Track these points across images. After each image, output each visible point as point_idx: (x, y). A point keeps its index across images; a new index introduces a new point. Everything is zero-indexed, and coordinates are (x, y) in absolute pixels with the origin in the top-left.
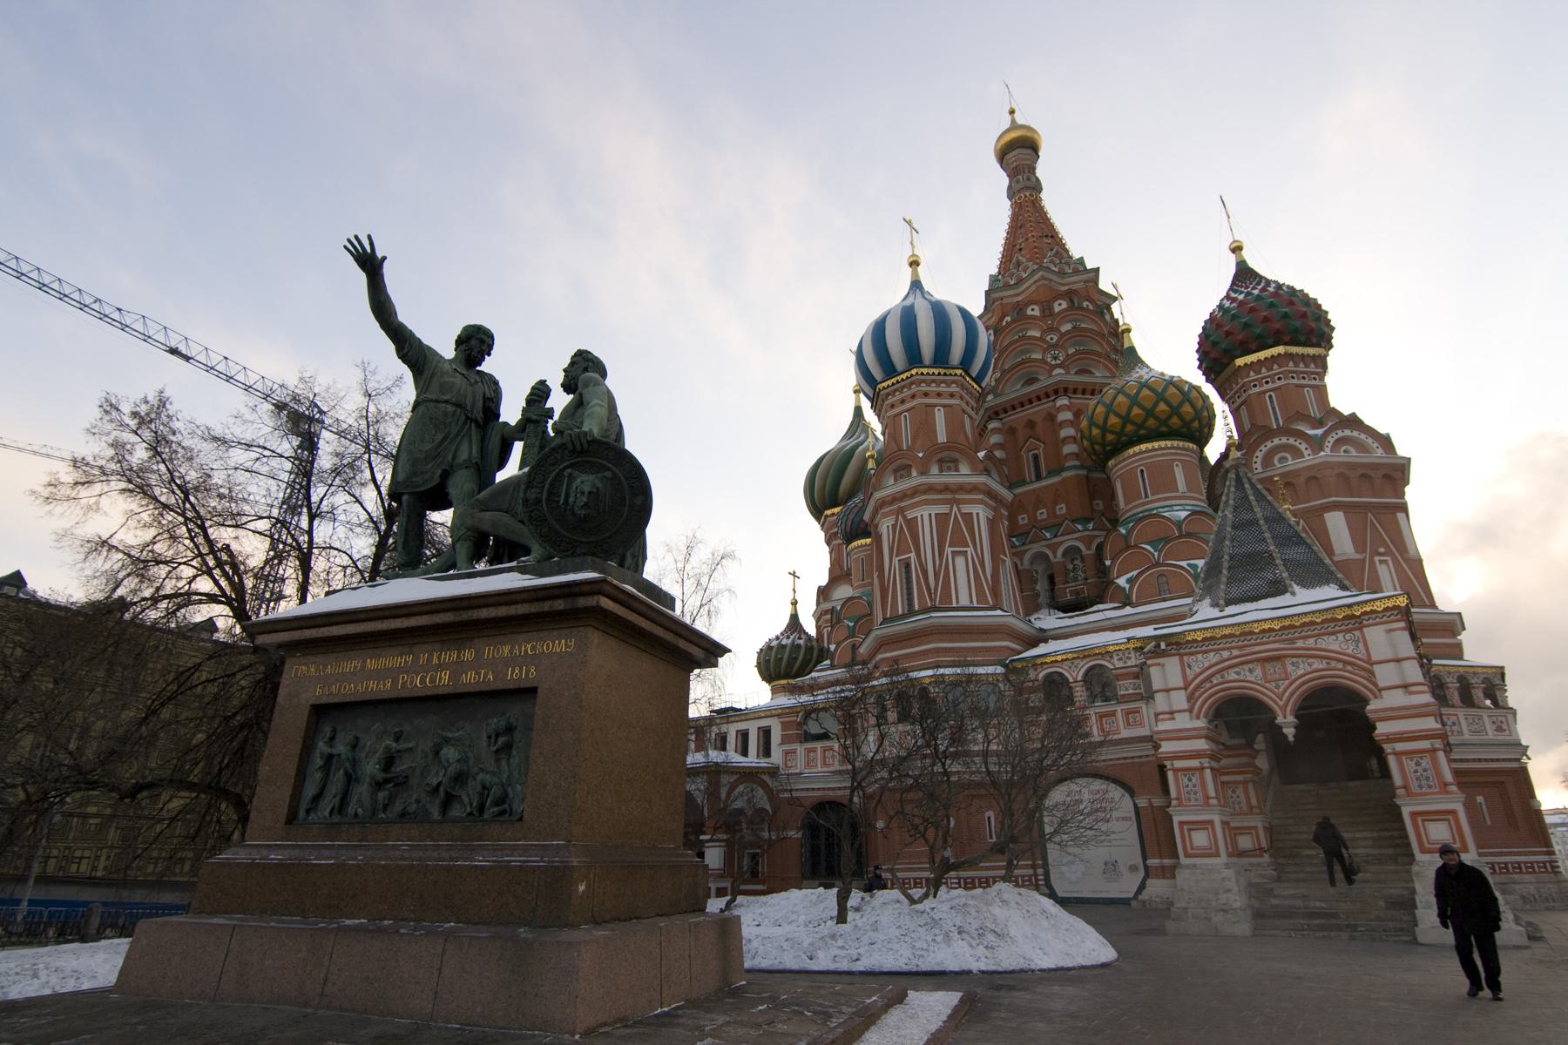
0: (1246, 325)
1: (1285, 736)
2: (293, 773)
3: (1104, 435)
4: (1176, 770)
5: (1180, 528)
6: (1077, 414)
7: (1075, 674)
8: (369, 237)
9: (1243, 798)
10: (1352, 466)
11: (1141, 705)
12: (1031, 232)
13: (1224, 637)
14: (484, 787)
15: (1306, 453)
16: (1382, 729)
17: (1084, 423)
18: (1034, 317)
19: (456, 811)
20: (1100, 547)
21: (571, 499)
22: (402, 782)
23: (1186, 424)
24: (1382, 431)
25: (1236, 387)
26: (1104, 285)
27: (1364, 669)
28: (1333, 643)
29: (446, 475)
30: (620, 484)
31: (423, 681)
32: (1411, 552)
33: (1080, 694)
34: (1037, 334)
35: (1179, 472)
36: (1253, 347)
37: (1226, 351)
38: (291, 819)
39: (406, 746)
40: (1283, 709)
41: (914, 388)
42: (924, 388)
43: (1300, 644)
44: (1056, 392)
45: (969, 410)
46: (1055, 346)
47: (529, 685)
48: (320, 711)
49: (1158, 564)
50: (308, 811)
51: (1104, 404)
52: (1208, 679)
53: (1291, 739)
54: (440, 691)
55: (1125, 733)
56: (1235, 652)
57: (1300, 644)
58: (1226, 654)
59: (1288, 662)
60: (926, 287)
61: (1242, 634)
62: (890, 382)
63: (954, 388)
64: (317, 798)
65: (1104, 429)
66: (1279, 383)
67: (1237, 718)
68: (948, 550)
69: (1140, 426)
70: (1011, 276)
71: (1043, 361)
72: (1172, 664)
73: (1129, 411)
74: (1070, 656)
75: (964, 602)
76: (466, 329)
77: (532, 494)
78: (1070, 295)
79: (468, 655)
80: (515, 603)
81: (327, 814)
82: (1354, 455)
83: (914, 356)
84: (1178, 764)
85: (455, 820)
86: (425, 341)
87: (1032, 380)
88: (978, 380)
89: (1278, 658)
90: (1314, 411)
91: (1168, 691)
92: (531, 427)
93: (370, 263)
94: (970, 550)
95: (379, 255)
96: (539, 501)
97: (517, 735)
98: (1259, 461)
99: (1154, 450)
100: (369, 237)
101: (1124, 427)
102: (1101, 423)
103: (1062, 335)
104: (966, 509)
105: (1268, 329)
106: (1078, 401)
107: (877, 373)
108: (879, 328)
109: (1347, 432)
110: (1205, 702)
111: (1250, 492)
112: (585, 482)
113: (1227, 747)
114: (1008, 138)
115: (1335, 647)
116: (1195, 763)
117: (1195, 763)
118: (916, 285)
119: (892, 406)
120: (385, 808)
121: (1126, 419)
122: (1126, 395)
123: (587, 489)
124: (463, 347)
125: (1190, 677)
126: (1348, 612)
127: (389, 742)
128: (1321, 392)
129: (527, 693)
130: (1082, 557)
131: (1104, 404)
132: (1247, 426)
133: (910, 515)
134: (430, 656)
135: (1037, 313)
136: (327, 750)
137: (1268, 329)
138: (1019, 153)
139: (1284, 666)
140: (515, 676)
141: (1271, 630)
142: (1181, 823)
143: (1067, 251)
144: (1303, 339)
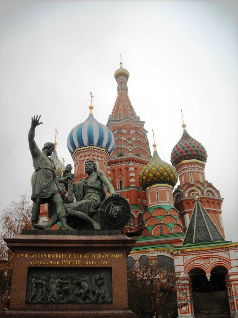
0: (186, 151)
1: (208, 280)
2: (25, 288)
3: (147, 179)
5: (167, 213)
6: (136, 169)
8: (40, 116)
10: (211, 199)
12: (123, 105)
14: (98, 294)
15: (200, 193)
16: (231, 278)
17: (141, 174)
18: (124, 133)
19: (88, 301)
20: (140, 215)
21: (112, 213)
22: (66, 293)
23: (171, 180)
24: (218, 190)
25: (181, 169)
26: (145, 127)
27: (228, 261)
28: (221, 254)
29: (53, 194)
30: (124, 210)
31: (71, 262)
32: (221, 226)
34: (125, 139)
35: (168, 194)
36: (188, 158)
37: (180, 158)
38: (27, 302)
39: (66, 281)
40: (208, 272)
41: (89, 153)
42: (93, 153)
43: (214, 254)
44: (130, 160)
45: (106, 162)
46: (131, 145)
47: (109, 266)
48: (32, 270)
49: (160, 224)
50: (32, 300)
51: (148, 169)
52: (190, 263)
53: (209, 280)
54: (78, 266)
56: (198, 255)
57: (214, 254)
58: (195, 256)
59: (210, 259)
60: (95, 117)
61: (200, 250)
62: (81, 149)
63: (103, 155)
64: (35, 296)
65: (148, 177)
66: (193, 170)
67: (196, 275)
69: (159, 178)
70: (117, 117)
71: (126, 149)
72: (181, 258)
73: (156, 173)
74: (136, 252)
76: (48, 144)
77: (103, 210)
78: (136, 128)
79: (87, 256)
80: (106, 243)
81: (40, 300)
82: (211, 196)
83: (91, 142)
85: (88, 303)
86: (38, 147)
87: (121, 155)
88: (109, 153)
89: (208, 258)
90: (201, 181)
91: (179, 266)
92: (69, 181)
93: (35, 123)
95: (39, 122)
96: (104, 212)
97: (105, 280)
98: (187, 193)
99: (162, 186)
100: (40, 116)
101: (154, 177)
102: (147, 175)
103: (133, 141)
105: (190, 153)
106: (137, 165)
107: (77, 144)
108: (79, 129)
109: (210, 189)
111: (201, 209)
112: (117, 208)
114: (120, 71)
115: (222, 256)
118: (91, 116)
119: (81, 157)
120: (62, 300)
121: (155, 175)
122: (155, 168)
123: (118, 210)
124: (47, 150)
125: (185, 262)
126: (226, 246)
128: (203, 174)
129: (109, 269)
130: (134, 218)
131: (148, 169)
132: (184, 183)
134: (73, 256)
135: (125, 132)
136: (37, 281)
137: (190, 153)
138: (122, 77)
139: (209, 260)
140: (103, 263)
141: (208, 250)
143: (135, 113)
144: (200, 158)
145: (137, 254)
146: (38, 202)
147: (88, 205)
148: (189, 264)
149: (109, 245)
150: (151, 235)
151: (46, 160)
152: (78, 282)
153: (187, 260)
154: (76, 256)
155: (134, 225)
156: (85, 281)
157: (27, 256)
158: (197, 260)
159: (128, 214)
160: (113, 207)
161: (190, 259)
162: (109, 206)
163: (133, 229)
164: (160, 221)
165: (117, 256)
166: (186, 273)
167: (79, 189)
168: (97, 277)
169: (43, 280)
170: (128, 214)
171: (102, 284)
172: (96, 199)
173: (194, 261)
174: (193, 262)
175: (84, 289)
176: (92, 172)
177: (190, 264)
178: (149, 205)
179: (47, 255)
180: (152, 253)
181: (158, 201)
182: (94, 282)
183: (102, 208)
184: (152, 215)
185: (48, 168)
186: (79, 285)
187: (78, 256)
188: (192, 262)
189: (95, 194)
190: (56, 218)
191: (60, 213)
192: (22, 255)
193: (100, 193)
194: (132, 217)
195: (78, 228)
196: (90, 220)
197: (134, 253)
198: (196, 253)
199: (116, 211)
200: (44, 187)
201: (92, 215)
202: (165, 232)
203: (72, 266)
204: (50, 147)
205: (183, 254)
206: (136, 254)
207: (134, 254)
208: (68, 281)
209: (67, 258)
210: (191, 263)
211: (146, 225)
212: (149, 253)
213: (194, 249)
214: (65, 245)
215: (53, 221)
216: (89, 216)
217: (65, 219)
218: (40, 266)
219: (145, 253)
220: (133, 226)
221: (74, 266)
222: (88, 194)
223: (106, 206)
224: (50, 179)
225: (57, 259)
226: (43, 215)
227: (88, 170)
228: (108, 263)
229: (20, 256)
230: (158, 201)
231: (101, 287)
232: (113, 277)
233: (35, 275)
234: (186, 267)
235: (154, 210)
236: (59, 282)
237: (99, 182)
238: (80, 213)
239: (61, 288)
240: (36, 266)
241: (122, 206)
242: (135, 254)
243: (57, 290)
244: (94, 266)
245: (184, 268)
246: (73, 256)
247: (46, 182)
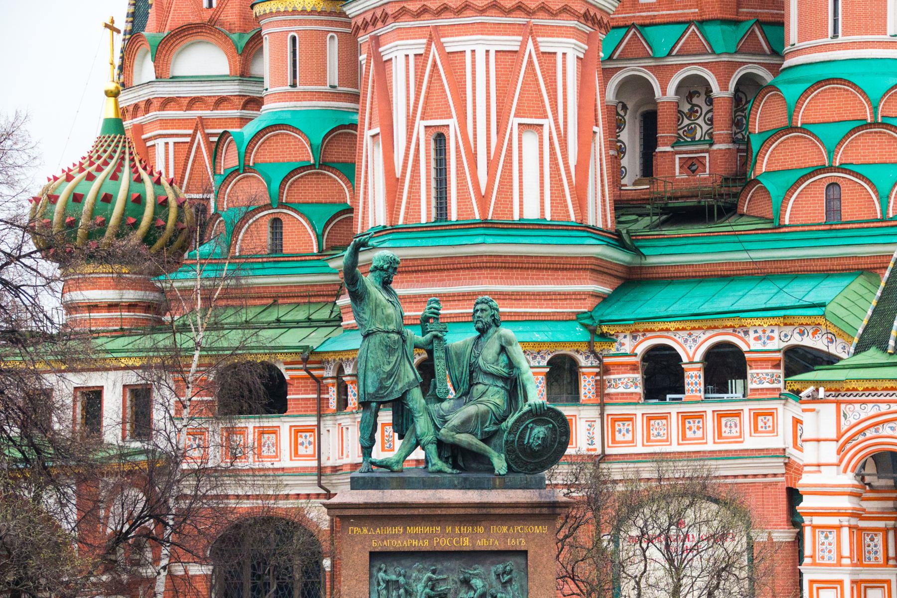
2: (367, 591)
4: (814, 527)
5: (874, 109)
7: (692, 349)
9: (880, 548)
11: (778, 405)
13: (886, 389)
21: (531, 441)
33: (694, 380)
39: (441, 577)
47: (523, 549)
48: (375, 556)
49: (831, 169)
52: (862, 432)
55: (751, 442)
58: (884, 408)
68: (514, 122)
75: (531, 213)
77: (511, 438)
79: (480, 530)
80: (517, 507)
84: (817, 521)
91: (818, 441)
92: (436, 342)
94: (548, 123)
96: (513, 441)
97: (514, 574)
104: (547, 44)
110: (854, 456)
112: (540, 431)
113: (873, 489)
116: (834, 521)
117: (834, 521)
123: (541, 436)
124: (383, 274)
125: (844, 428)
127: (430, 574)
130: (710, 101)
133: (452, 44)
134: (453, 530)
136: (387, 578)
140: (512, 544)
142: (812, 582)
145: (696, 333)
146: (373, 410)
147: (482, 417)
148: (861, 438)
149: (522, 511)
150: (780, 226)
151: (385, 306)
152: (464, 578)
153: (854, 422)
154: (460, 530)
155: (711, 145)
156: (477, 576)
157: (365, 530)
158: (892, 424)
159: (563, 439)
160: (532, 429)
161: (863, 416)
162: (523, 429)
163: (700, 160)
164: (831, 153)
165: (538, 529)
166: (845, 471)
167: (458, 360)
168: (500, 567)
169: (399, 575)
170: (563, 439)
171: (510, 581)
172: (498, 401)
173: (880, 427)
174: (877, 431)
175: (475, 591)
176: (488, 329)
177: (865, 434)
178: (787, 49)
179: (405, 529)
180: (760, 333)
181: (835, 36)
182: (493, 577)
183: (509, 433)
184: (791, 117)
185: (391, 327)
186: (466, 583)
187: (464, 529)
188: (873, 429)
189: (496, 389)
190: (413, 441)
191: (423, 434)
192: (356, 529)
193: (506, 384)
194: (703, 92)
195: (461, 464)
196: (485, 451)
197: (678, 329)
198: (888, 398)
199: (539, 438)
200: (385, 376)
201: (487, 439)
202: (850, 210)
203: (453, 549)
204: (388, 268)
205: (840, 398)
206: (690, 335)
207: (681, 333)
208: (445, 576)
209: (444, 534)
210: (869, 434)
211: (763, 166)
212: (746, 333)
213: (880, 383)
214: (439, 512)
215: (409, 446)
216: (482, 440)
217: (434, 446)
218: (392, 549)
219: (730, 331)
220: (707, 147)
221: (457, 549)
222: (480, 387)
223: (518, 429)
224: (396, 355)
225: (426, 536)
226: (199, 38)
227: (480, 325)
228: (520, 543)
229: (352, 531)
230: (835, 36)
231: (506, 587)
232: (530, 570)
233: (383, 566)
234: (848, 446)
235: (806, 93)
236: (430, 579)
237: (503, 358)
238: (464, 438)
239: (432, 589)
240: (384, 549)
241: (551, 426)
242: (684, 334)
243: (427, 594)
244: (494, 549)
245: (838, 453)
246: (453, 530)
247: (389, 363)
